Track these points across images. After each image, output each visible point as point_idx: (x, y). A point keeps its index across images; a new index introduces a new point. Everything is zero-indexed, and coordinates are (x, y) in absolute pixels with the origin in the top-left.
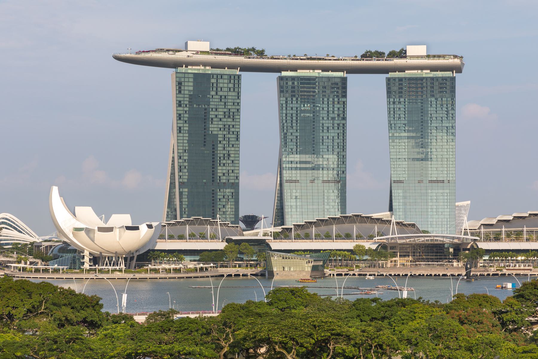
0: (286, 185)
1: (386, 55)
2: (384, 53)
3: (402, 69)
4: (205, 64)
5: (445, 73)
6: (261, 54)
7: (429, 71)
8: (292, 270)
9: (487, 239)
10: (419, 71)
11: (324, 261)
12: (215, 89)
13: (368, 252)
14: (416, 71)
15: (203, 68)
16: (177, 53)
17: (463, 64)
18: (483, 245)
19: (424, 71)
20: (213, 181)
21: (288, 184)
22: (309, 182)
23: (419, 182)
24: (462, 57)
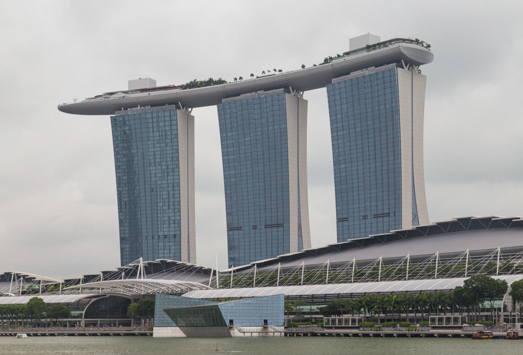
6: (220, 82)
15: (142, 108)
22: (251, 228)
23: (365, 217)
24: (417, 41)
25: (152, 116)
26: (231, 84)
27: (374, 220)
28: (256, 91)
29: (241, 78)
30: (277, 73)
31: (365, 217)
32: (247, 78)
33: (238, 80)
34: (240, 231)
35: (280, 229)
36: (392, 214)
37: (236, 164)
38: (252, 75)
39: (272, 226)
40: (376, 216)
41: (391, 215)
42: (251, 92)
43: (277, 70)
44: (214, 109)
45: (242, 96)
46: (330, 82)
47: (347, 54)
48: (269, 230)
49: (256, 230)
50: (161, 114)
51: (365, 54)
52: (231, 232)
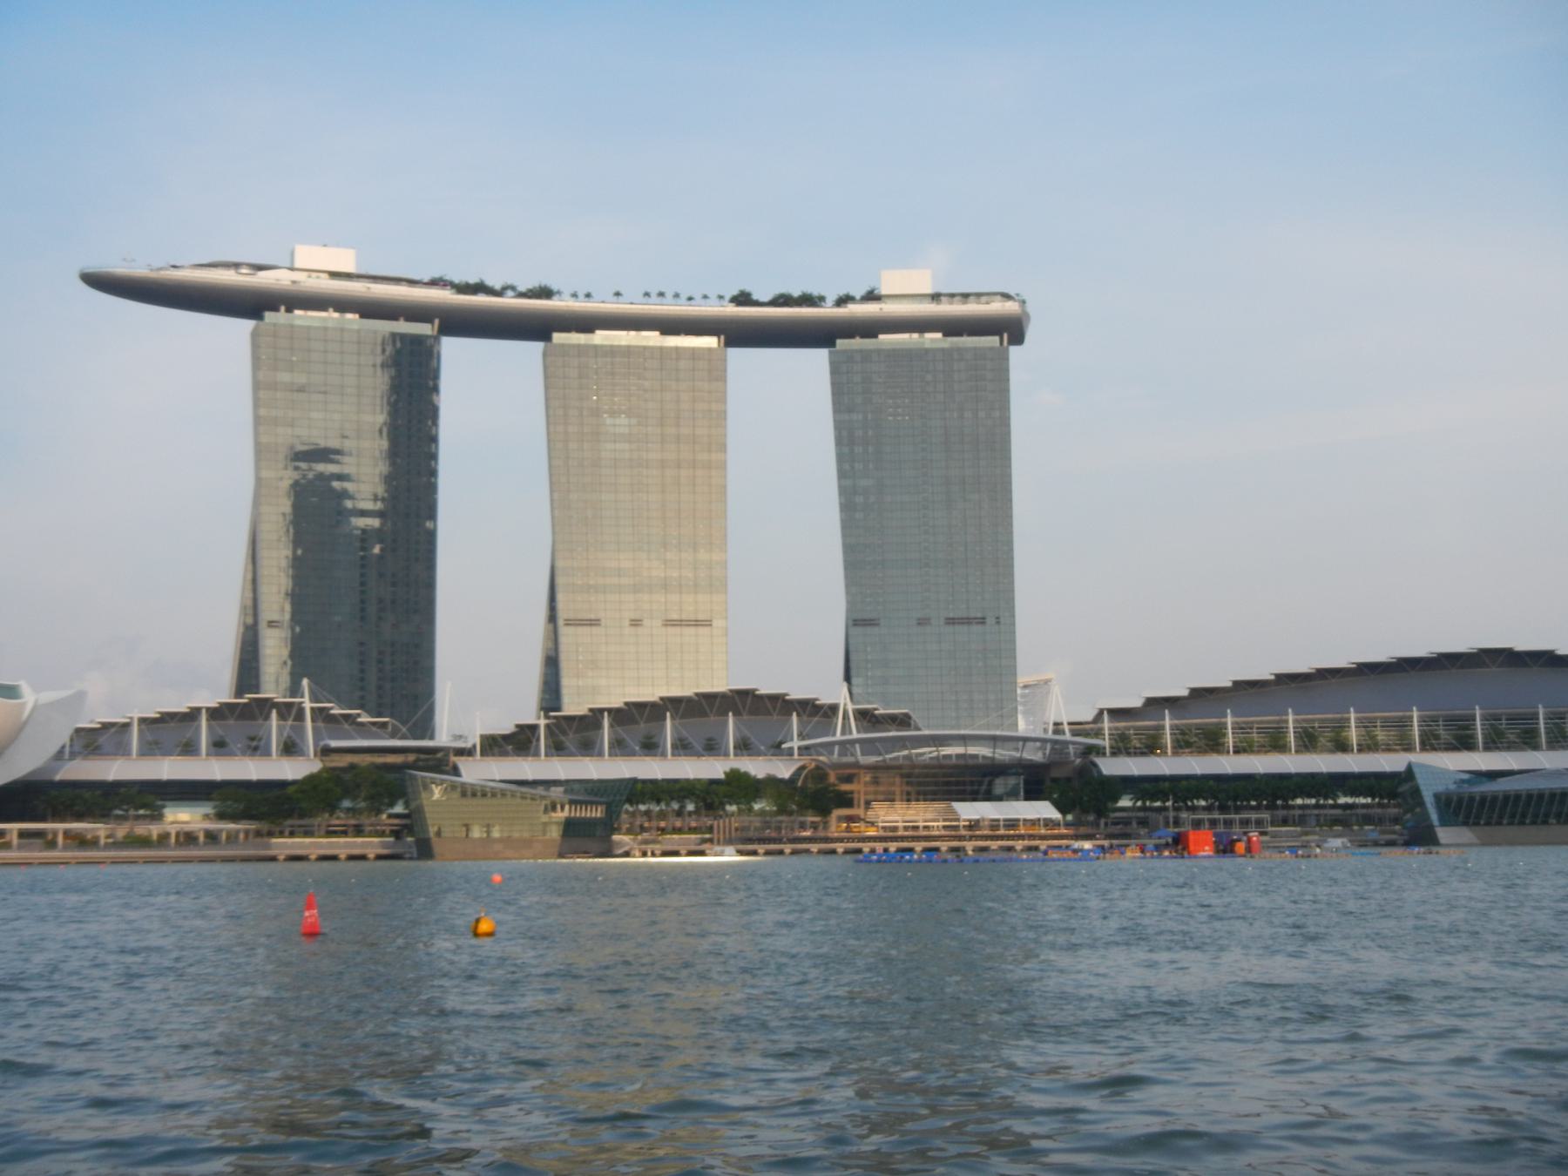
0: (567, 635)
1: (830, 300)
2: (822, 299)
3: (870, 329)
4: (342, 304)
5: (983, 339)
7: (939, 335)
8: (496, 834)
9: (1122, 747)
10: (915, 336)
11: (609, 806)
13: (771, 785)
14: (906, 336)
15: (336, 315)
16: (262, 274)
17: (1027, 316)
18: (1111, 767)
19: (929, 336)
20: (362, 618)
21: (571, 630)
22: (627, 623)
23: (923, 622)
27: (950, 629)
31: (923, 622)
33: (581, 296)
34: (595, 630)
35: (701, 630)
36: (990, 620)
38: (618, 294)
39: (680, 623)
40: (951, 621)
41: (988, 621)
43: (684, 297)
45: (601, 337)
46: (833, 344)
48: (671, 630)
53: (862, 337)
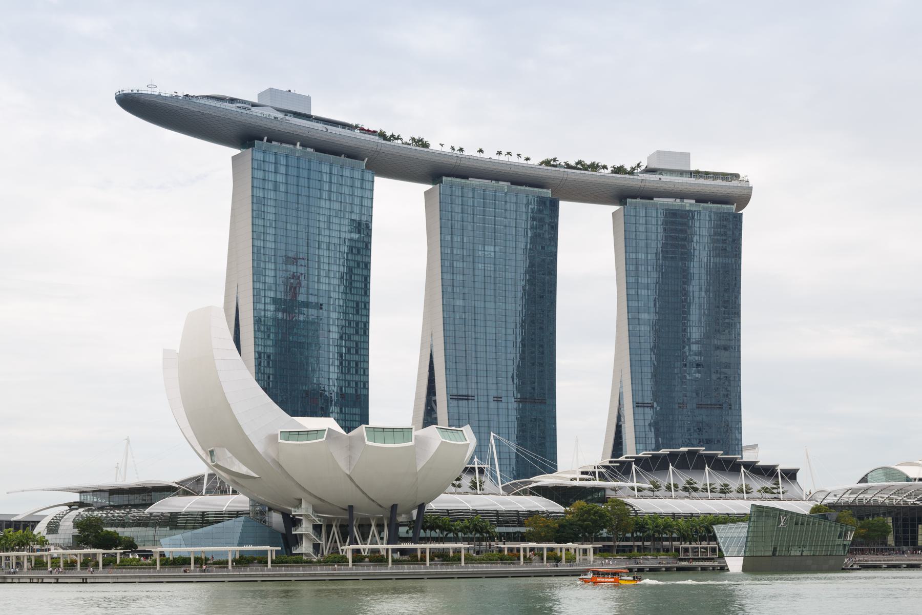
7: (694, 201)
10: (678, 200)
12: (325, 195)
19: (685, 201)
22: (491, 399)
25: (331, 170)
26: (435, 153)
28: (497, 180)
29: (461, 150)
30: (522, 161)
32: (471, 152)
37: (466, 290)
38: (481, 151)
42: (491, 179)
43: (524, 156)
44: (420, 189)
45: (472, 181)
47: (649, 171)
49: (500, 404)
50: (347, 172)
51: (692, 180)
52: (455, 402)
53: (642, 198)
